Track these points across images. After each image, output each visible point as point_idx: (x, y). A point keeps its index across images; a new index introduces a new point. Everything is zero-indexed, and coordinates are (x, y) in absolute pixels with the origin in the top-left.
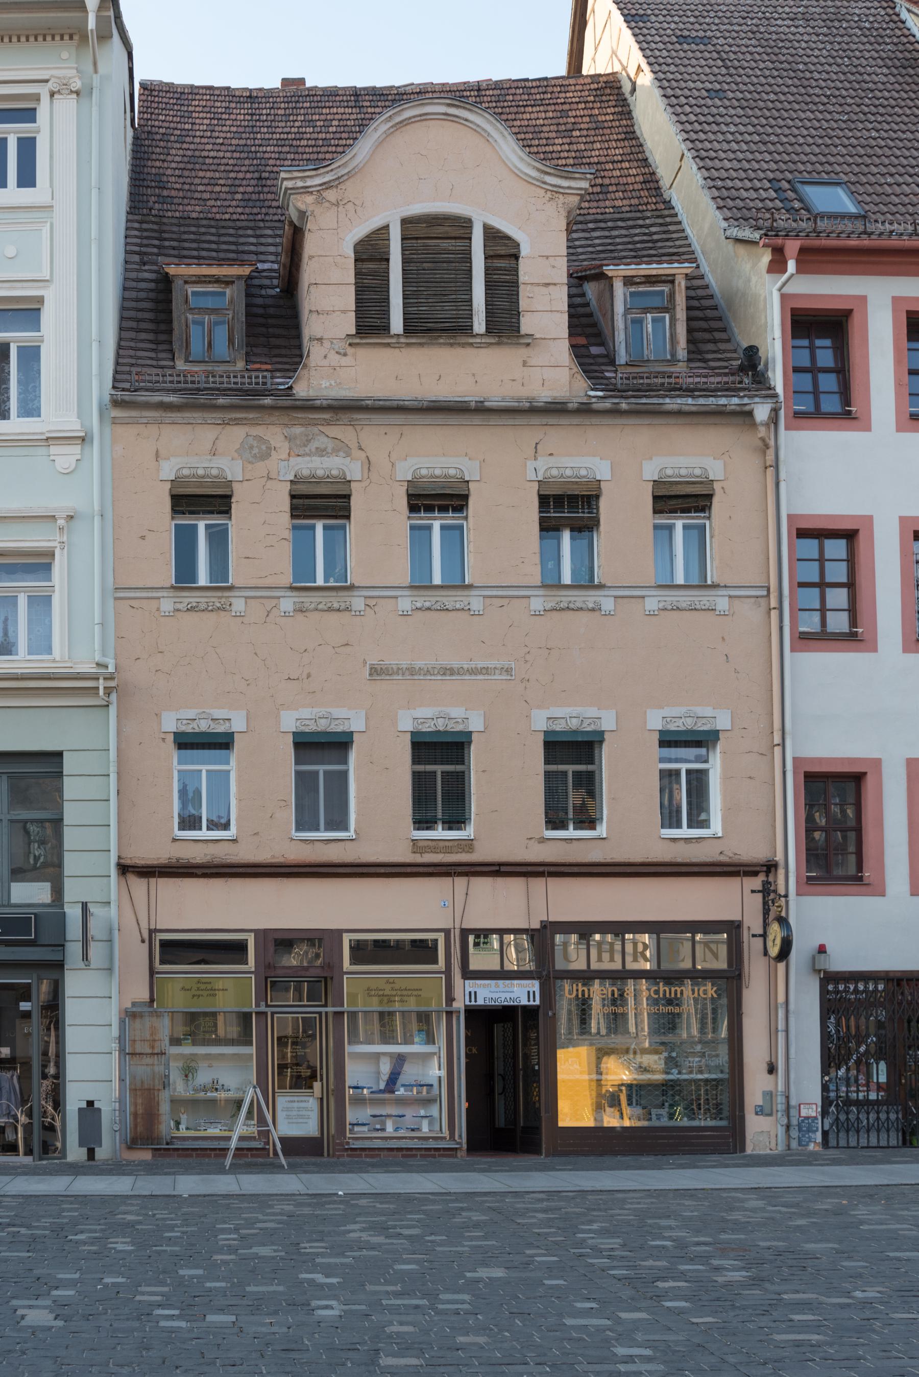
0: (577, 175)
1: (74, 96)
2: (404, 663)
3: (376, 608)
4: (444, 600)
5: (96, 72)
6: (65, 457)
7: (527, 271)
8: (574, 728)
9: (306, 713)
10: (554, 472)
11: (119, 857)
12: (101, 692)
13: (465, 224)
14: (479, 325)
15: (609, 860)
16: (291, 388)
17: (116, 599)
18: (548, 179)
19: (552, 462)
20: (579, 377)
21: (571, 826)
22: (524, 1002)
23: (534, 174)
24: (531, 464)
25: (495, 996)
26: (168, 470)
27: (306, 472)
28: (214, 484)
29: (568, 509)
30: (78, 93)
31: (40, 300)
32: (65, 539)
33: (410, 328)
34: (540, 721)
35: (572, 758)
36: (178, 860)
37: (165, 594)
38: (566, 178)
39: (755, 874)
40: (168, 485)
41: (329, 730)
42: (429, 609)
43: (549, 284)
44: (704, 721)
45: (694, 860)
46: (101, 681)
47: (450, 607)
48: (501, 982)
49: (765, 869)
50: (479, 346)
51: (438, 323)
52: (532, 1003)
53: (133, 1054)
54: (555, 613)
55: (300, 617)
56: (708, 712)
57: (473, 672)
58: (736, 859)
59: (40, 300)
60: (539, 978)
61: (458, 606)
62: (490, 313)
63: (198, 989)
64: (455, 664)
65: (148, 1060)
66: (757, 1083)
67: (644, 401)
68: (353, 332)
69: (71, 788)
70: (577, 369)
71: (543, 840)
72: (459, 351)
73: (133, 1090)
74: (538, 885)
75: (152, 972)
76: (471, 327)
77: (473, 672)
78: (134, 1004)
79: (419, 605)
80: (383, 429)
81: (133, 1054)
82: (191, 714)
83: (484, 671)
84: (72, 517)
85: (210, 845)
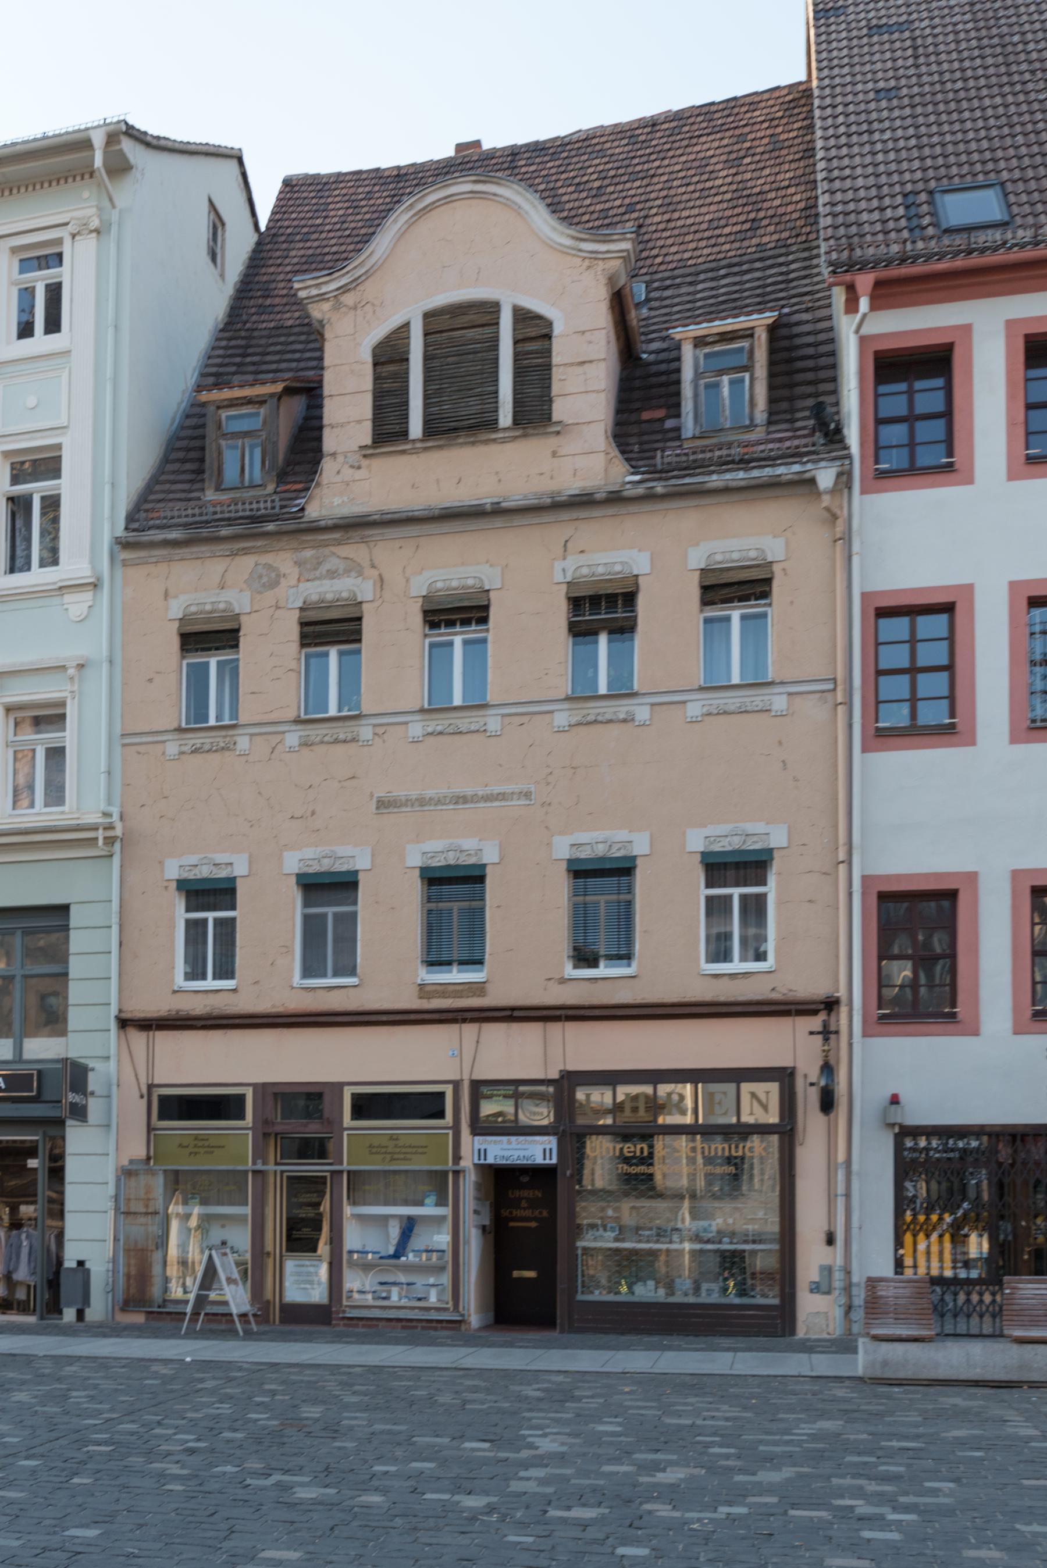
2: (414, 794)
3: (385, 736)
7: (561, 352)
8: (601, 854)
9: (309, 853)
11: (120, 1011)
22: (539, 1160)
24: (558, 566)
25: (507, 1153)
34: (563, 849)
36: (178, 1012)
37: (170, 737)
39: (815, 1012)
42: (441, 733)
45: (741, 998)
48: (513, 1138)
49: (822, 1006)
51: (460, 418)
52: (547, 1161)
53: (127, 1213)
56: (760, 827)
58: (790, 996)
60: (554, 1134)
61: (473, 728)
62: (517, 403)
63: (195, 1146)
69: (77, 941)
71: (563, 981)
74: (555, 1029)
75: (150, 1129)
78: (131, 1162)
79: (430, 730)
81: (127, 1213)
82: (193, 859)
85: (211, 995)
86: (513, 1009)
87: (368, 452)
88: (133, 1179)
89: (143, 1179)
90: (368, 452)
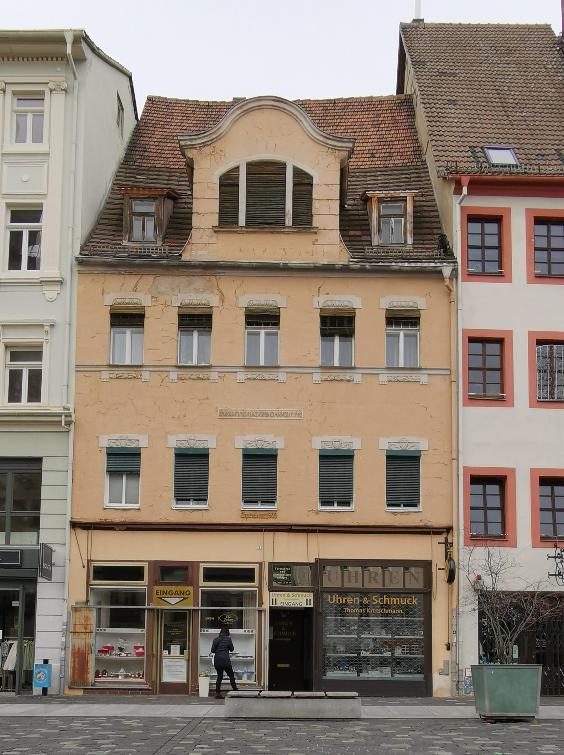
0: (345, 140)
1: (64, 92)
2: (240, 409)
4: (264, 374)
5: (75, 78)
6: (51, 292)
8: (337, 448)
9: (182, 437)
11: (72, 518)
12: (63, 424)
13: (282, 166)
14: (289, 221)
15: (356, 524)
16: (181, 255)
17: (76, 371)
18: (329, 142)
19: (328, 297)
20: (344, 250)
21: (336, 505)
23: (321, 139)
26: (109, 300)
27: (187, 302)
29: (337, 325)
30: (66, 91)
31: (41, 205)
33: (249, 222)
37: (104, 369)
38: (339, 141)
39: (441, 533)
40: (109, 308)
41: (194, 447)
42: (254, 379)
43: (328, 200)
44: (412, 445)
45: (406, 525)
46: (63, 417)
47: (267, 378)
48: (291, 593)
49: (445, 530)
50: (288, 233)
51: (265, 220)
52: (308, 606)
54: (327, 382)
57: (278, 415)
58: (429, 524)
59: (41, 205)
60: (312, 592)
61: (271, 378)
66: (440, 656)
67: (381, 264)
68: (217, 224)
70: (343, 246)
71: (318, 512)
73: (74, 654)
74: (313, 538)
75: (88, 584)
76: (284, 223)
77: (278, 415)
78: (76, 603)
79: (249, 377)
80: (232, 278)
82: (117, 436)
83: (285, 415)
84: (53, 325)
86: (291, 525)
87: (216, 230)
88: (78, 613)
89: (84, 613)
90: (216, 230)
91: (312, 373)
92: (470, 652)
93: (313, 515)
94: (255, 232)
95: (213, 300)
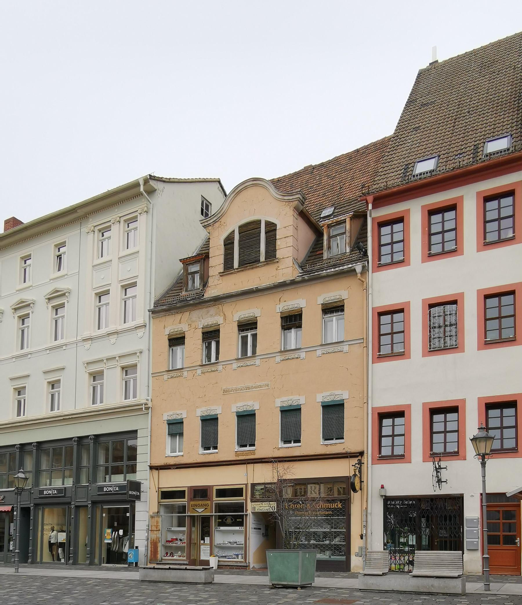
10: (286, 308)
21: (292, 442)
28: (180, 334)
32: (139, 359)
35: (291, 415)
55: (203, 375)
64: (250, 384)
65: (155, 532)
72: (255, 270)
80: (230, 304)
91: (275, 357)
92: (377, 539)
93: (276, 450)
94: (242, 271)
95: (219, 320)
